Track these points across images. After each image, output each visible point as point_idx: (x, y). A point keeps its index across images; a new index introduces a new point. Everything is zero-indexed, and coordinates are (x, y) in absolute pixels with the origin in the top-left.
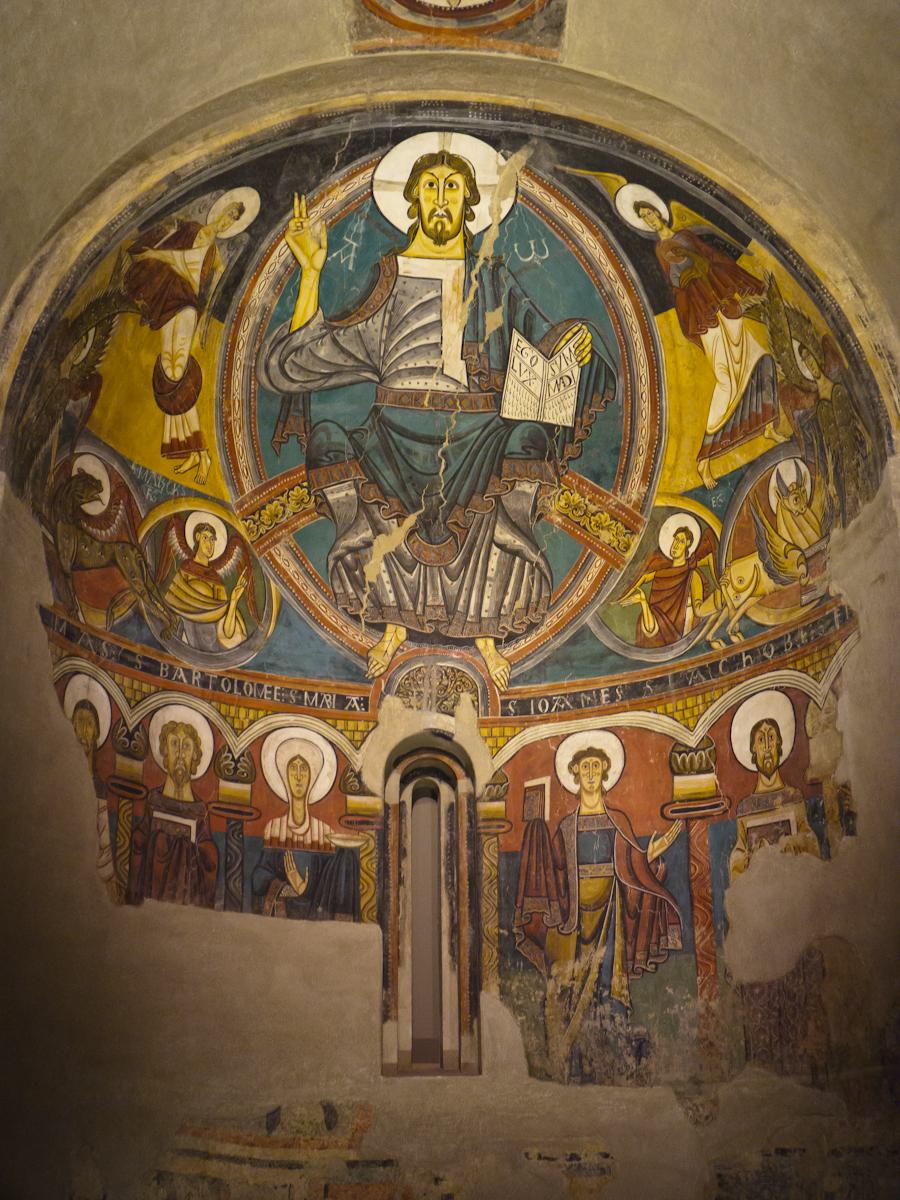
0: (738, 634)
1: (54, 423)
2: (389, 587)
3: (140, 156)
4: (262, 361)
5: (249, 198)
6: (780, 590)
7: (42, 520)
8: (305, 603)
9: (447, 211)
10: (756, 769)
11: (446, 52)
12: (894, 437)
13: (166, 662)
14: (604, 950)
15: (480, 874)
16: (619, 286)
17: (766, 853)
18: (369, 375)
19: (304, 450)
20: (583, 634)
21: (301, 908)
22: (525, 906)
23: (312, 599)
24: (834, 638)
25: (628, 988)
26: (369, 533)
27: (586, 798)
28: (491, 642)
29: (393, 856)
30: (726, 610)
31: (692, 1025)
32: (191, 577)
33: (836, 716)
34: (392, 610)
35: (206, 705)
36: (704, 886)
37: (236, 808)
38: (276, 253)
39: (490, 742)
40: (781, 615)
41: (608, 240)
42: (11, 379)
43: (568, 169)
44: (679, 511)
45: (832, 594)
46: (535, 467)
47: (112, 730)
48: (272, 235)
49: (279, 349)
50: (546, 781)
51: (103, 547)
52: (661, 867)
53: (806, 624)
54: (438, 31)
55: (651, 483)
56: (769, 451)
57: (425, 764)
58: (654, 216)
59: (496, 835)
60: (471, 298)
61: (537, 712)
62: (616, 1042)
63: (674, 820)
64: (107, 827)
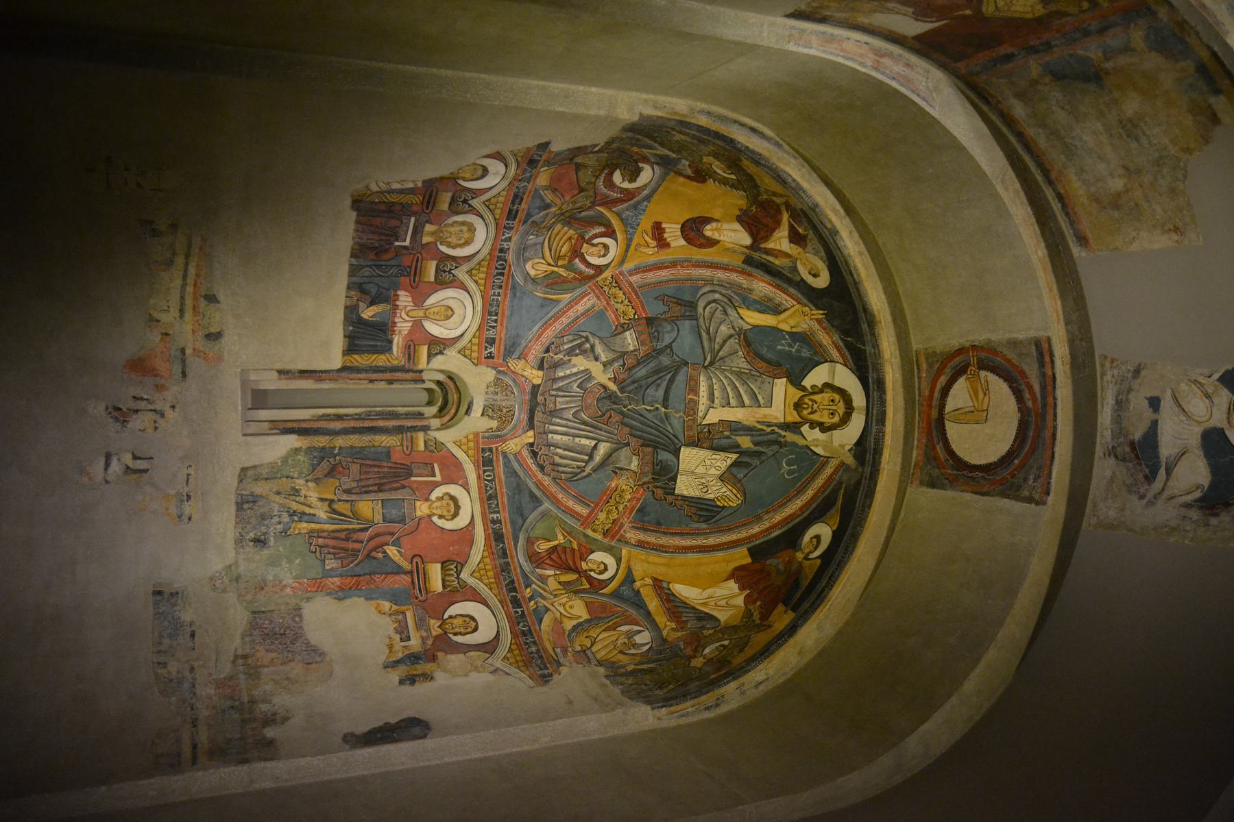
0: (535, 606)
1: (673, 152)
2: (568, 372)
3: (849, 210)
4: (717, 288)
5: (822, 281)
6: (564, 633)
7: (609, 143)
8: (557, 317)
9: (816, 411)
10: (445, 618)
11: (917, 411)
12: (664, 709)
13: (516, 225)
14: (325, 517)
15: (375, 434)
16: (765, 525)
17: (387, 626)
18: (709, 359)
19: (659, 316)
20: (536, 501)
21: (352, 316)
22: (353, 464)
23: (560, 321)
24: (531, 670)
25: (299, 534)
26: (603, 358)
27: (427, 504)
28: (531, 440)
29: (388, 376)
30: (552, 597)
31: (275, 576)
32: (573, 241)
33: (479, 672)
34: (552, 374)
35: (487, 251)
36: (367, 584)
37: (418, 272)
38: (788, 298)
39: (464, 440)
40: (548, 634)
41: (797, 518)
42: (700, 124)
43: (842, 491)
44: (618, 565)
45: (561, 668)
46: (647, 469)
47: (469, 190)
48: (800, 296)
49: (725, 300)
50: (438, 478)
51: (591, 183)
52: (380, 555)
53: (541, 651)
54: (930, 406)
55: (638, 546)
56: (657, 625)
57: (450, 396)
58: (812, 548)
59: (402, 445)
60: (759, 427)
61: (485, 471)
62: (264, 525)
63: (411, 563)
64: (403, 187)
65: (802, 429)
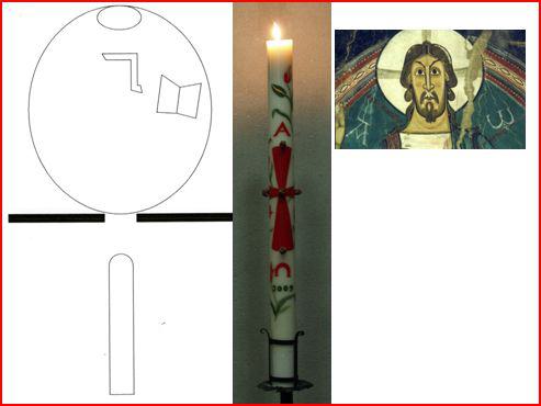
9: (434, 94)
65: (456, 109)
